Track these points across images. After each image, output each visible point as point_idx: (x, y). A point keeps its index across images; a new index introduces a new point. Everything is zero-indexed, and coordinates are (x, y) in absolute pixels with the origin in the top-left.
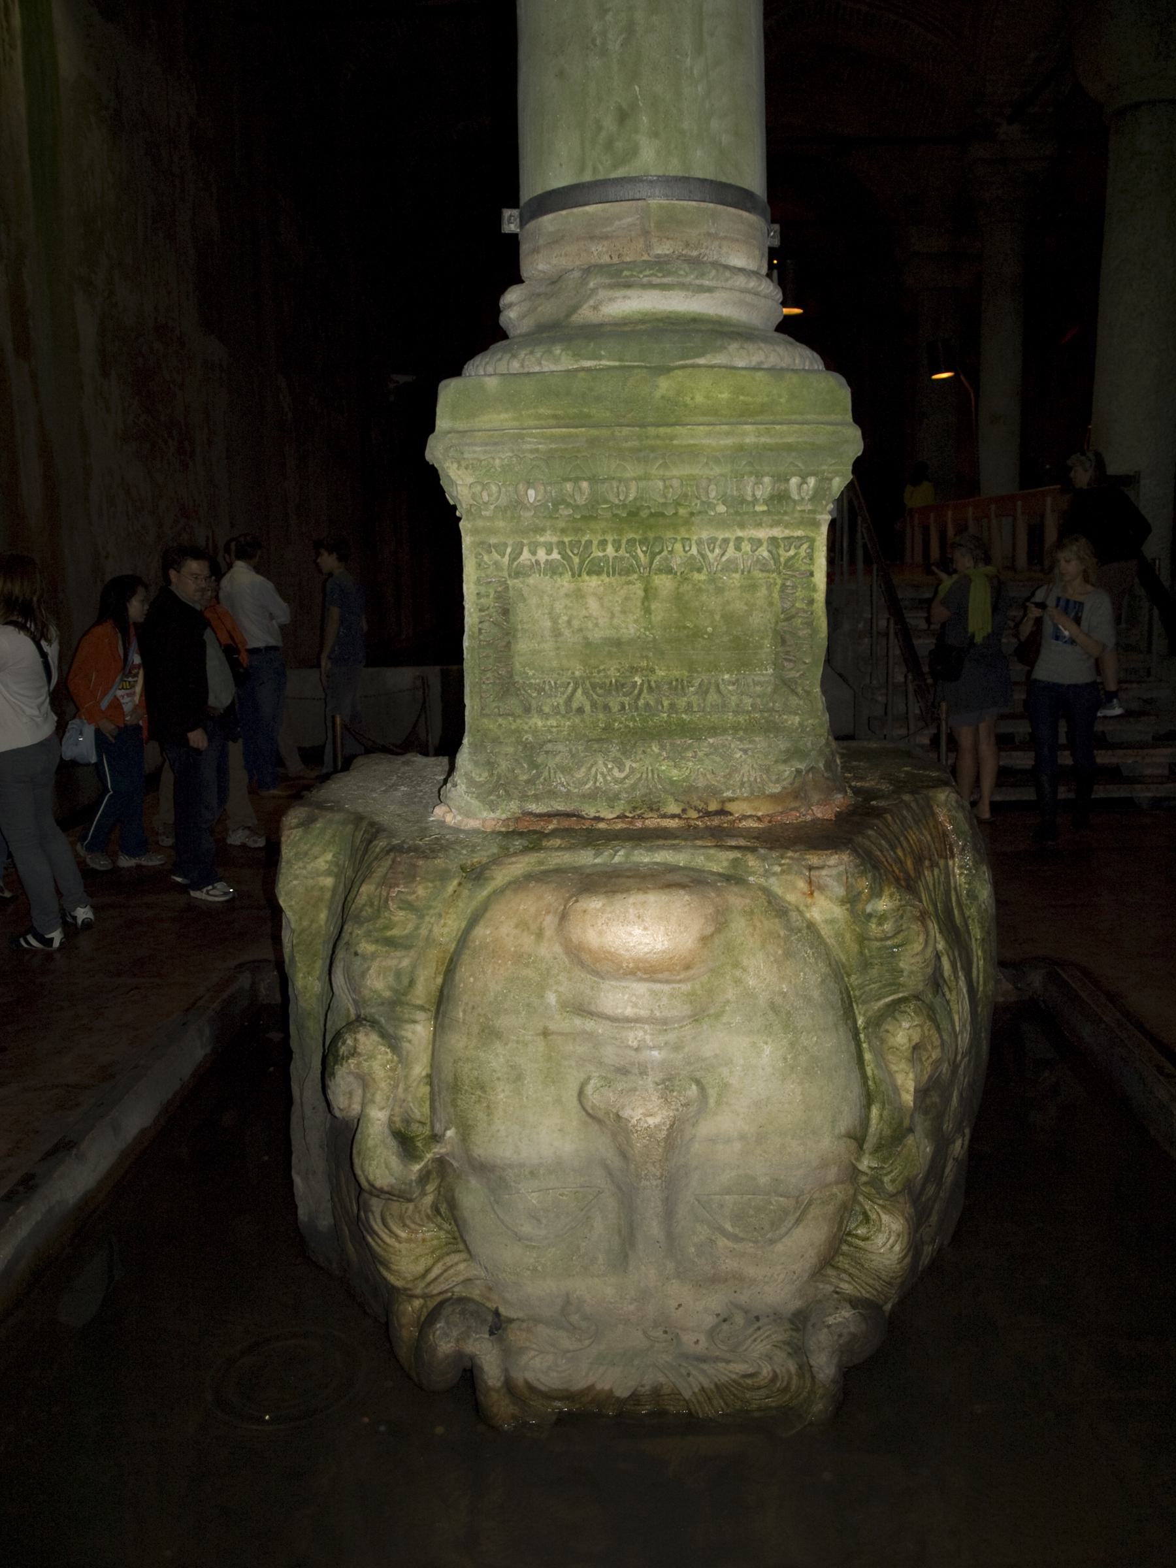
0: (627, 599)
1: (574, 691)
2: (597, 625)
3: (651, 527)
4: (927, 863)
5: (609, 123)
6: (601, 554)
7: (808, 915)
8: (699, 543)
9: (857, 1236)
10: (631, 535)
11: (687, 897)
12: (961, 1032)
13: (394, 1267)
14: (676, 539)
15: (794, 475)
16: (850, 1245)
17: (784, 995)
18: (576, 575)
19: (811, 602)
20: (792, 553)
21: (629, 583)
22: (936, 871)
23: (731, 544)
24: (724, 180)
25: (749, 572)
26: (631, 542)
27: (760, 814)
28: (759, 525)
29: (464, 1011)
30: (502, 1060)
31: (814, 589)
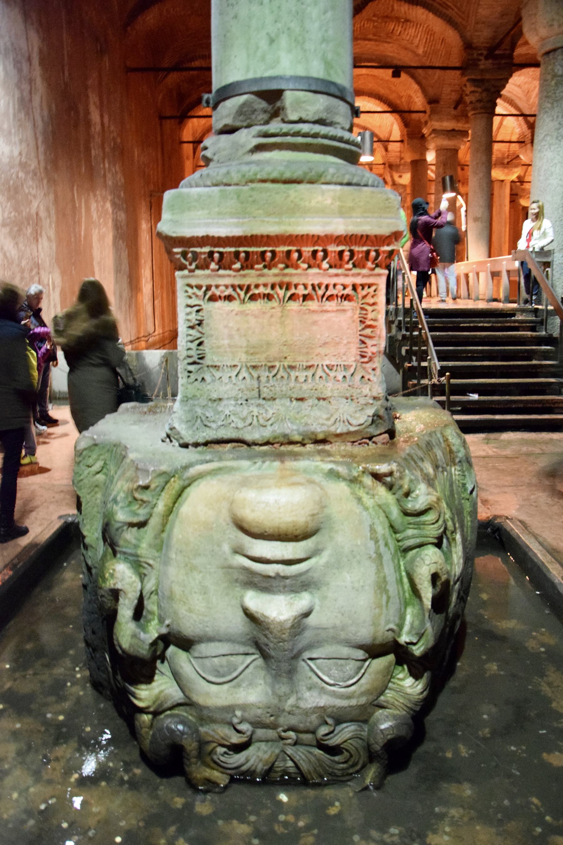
2: (253, 333)
4: (440, 469)
5: (264, 44)
8: (313, 285)
9: (398, 679)
11: (304, 491)
12: (458, 563)
13: (138, 696)
16: (394, 683)
17: (357, 546)
18: (243, 302)
22: (445, 473)
23: (331, 287)
24: (329, 79)
28: (347, 275)
29: (176, 554)
30: (197, 581)
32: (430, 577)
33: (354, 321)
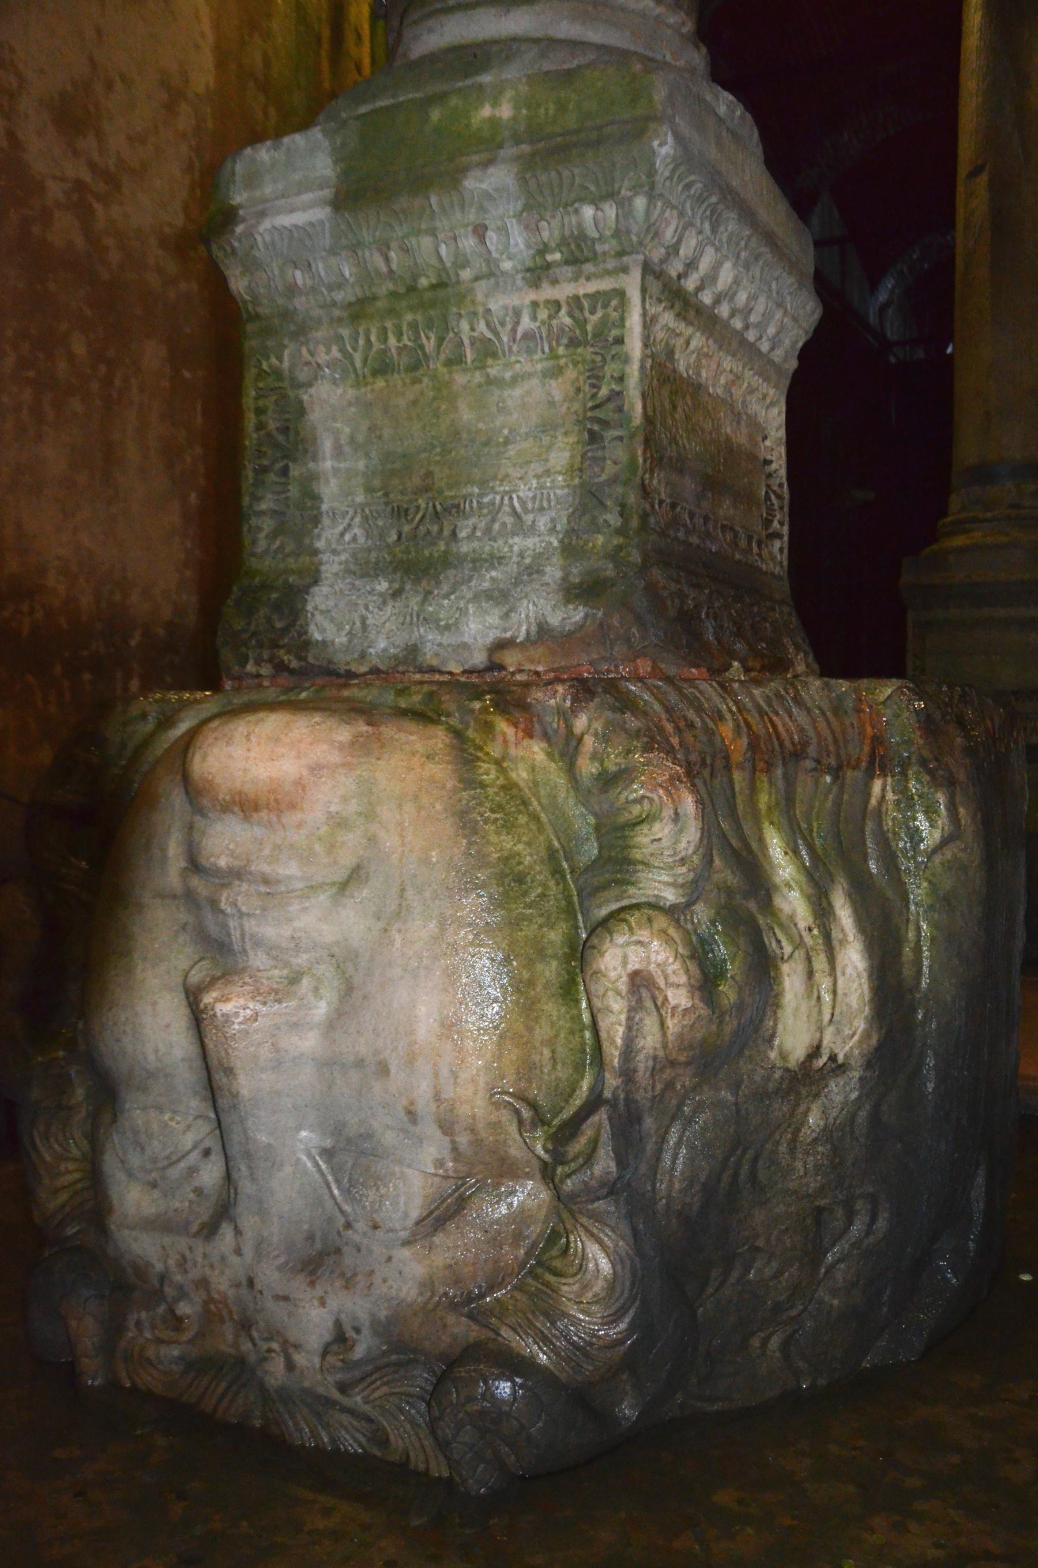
0: (415, 403)
1: (352, 519)
3: (433, 304)
6: (383, 347)
7: (513, 775)
10: (409, 317)
14: (460, 315)
15: (581, 200)
19: (621, 379)
20: (599, 314)
21: (416, 381)
25: (551, 348)
26: (414, 326)
27: (540, 668)
28: (555, 282)
31: (626, 360)
32: (625, 979)
33: (578, 390)
